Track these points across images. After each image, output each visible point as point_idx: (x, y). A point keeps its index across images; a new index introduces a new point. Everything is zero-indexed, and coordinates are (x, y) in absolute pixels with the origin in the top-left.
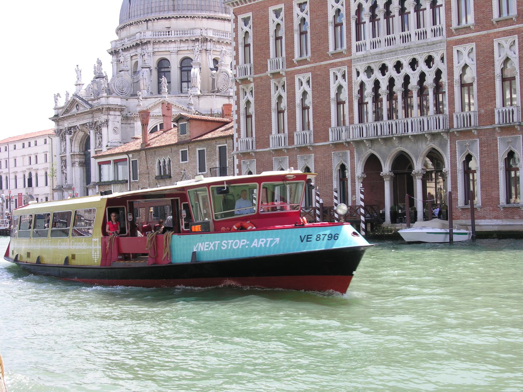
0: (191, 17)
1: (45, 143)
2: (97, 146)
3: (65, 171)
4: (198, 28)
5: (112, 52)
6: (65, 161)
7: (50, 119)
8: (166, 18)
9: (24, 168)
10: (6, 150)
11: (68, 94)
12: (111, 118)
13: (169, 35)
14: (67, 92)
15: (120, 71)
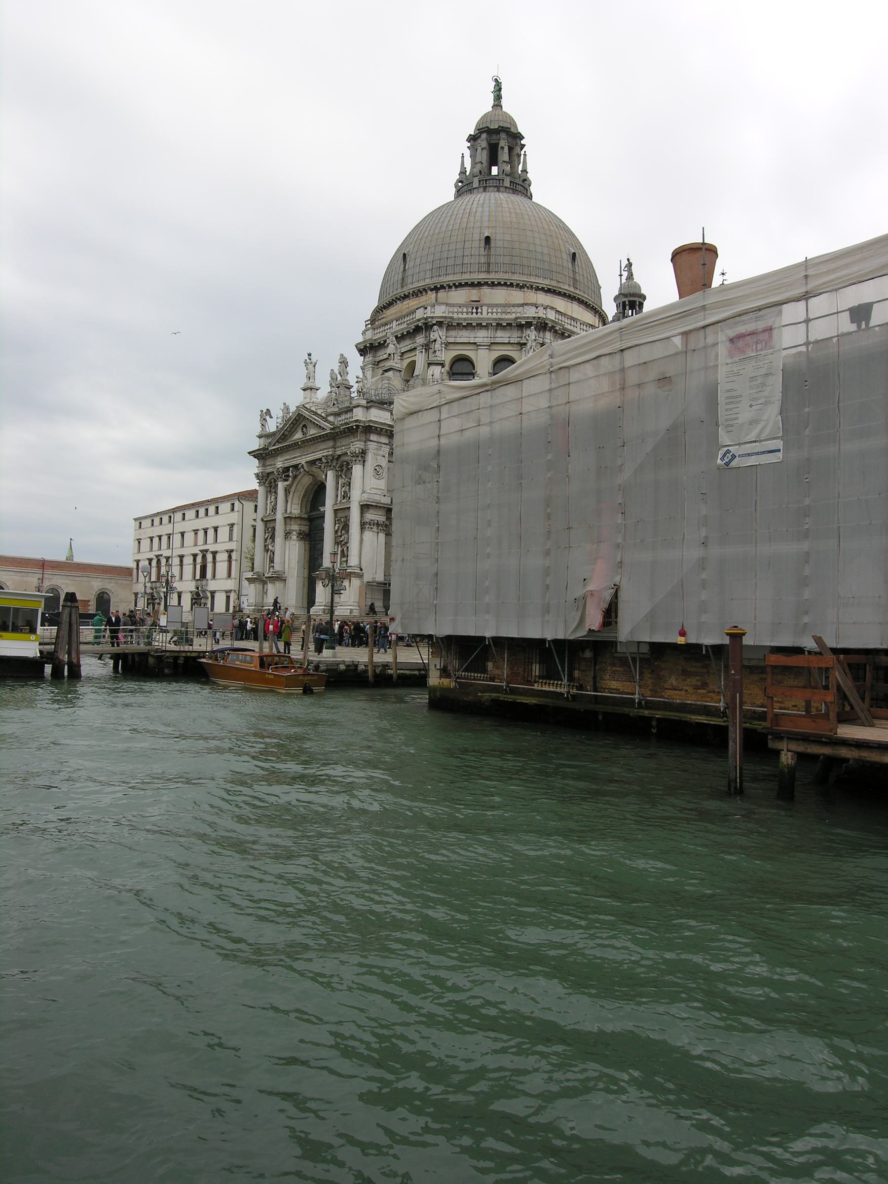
0: (518, 285)
1: (233, 510)
2: (339, 500)
3: (270, 547)
4: (532, 305)
5: (365, 347)
6: (274, 529)
7: (249, 453)
8: (472, 285)
9: (196, 550)
10: (170, 522)
11: (286, 408)
12: (372, 446)
13: (477, 313)
14: (285, 404)
15: (386, 371)
